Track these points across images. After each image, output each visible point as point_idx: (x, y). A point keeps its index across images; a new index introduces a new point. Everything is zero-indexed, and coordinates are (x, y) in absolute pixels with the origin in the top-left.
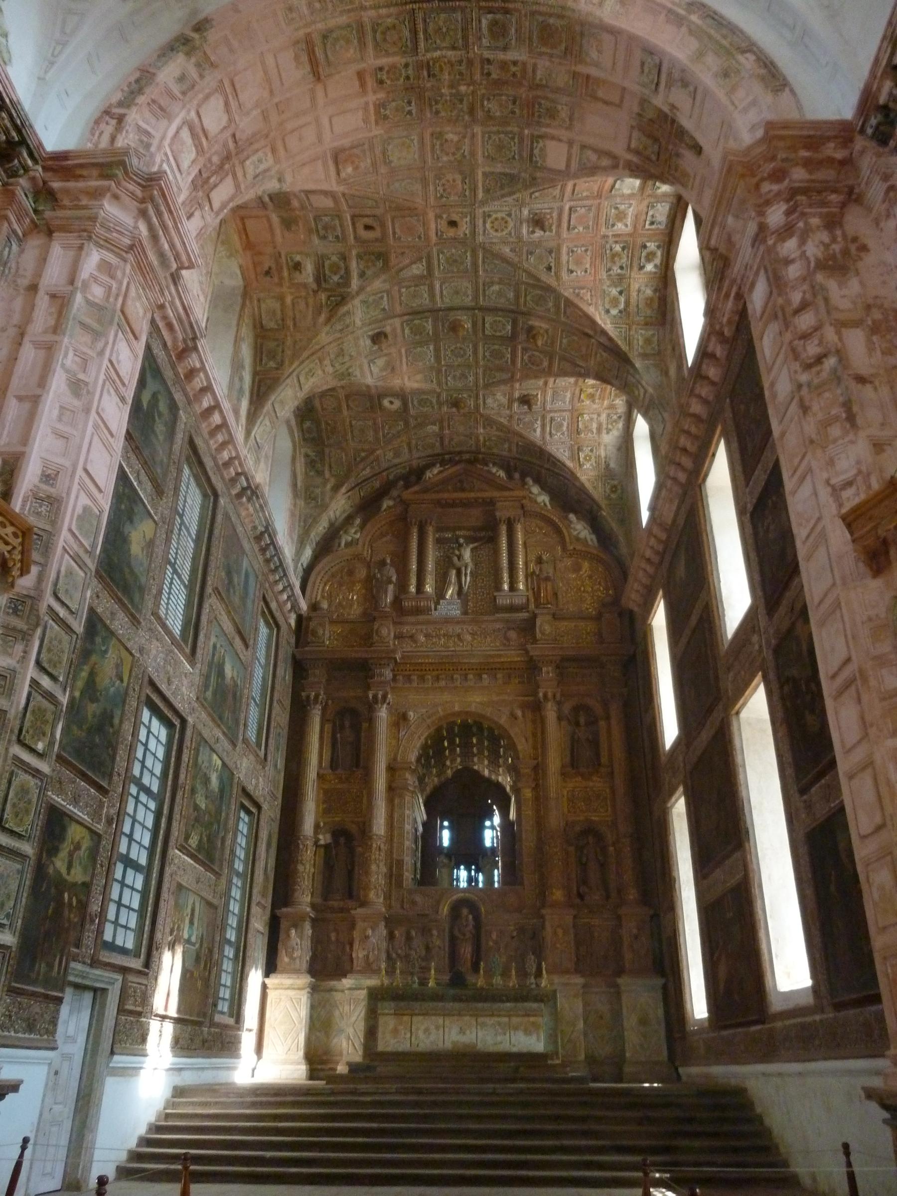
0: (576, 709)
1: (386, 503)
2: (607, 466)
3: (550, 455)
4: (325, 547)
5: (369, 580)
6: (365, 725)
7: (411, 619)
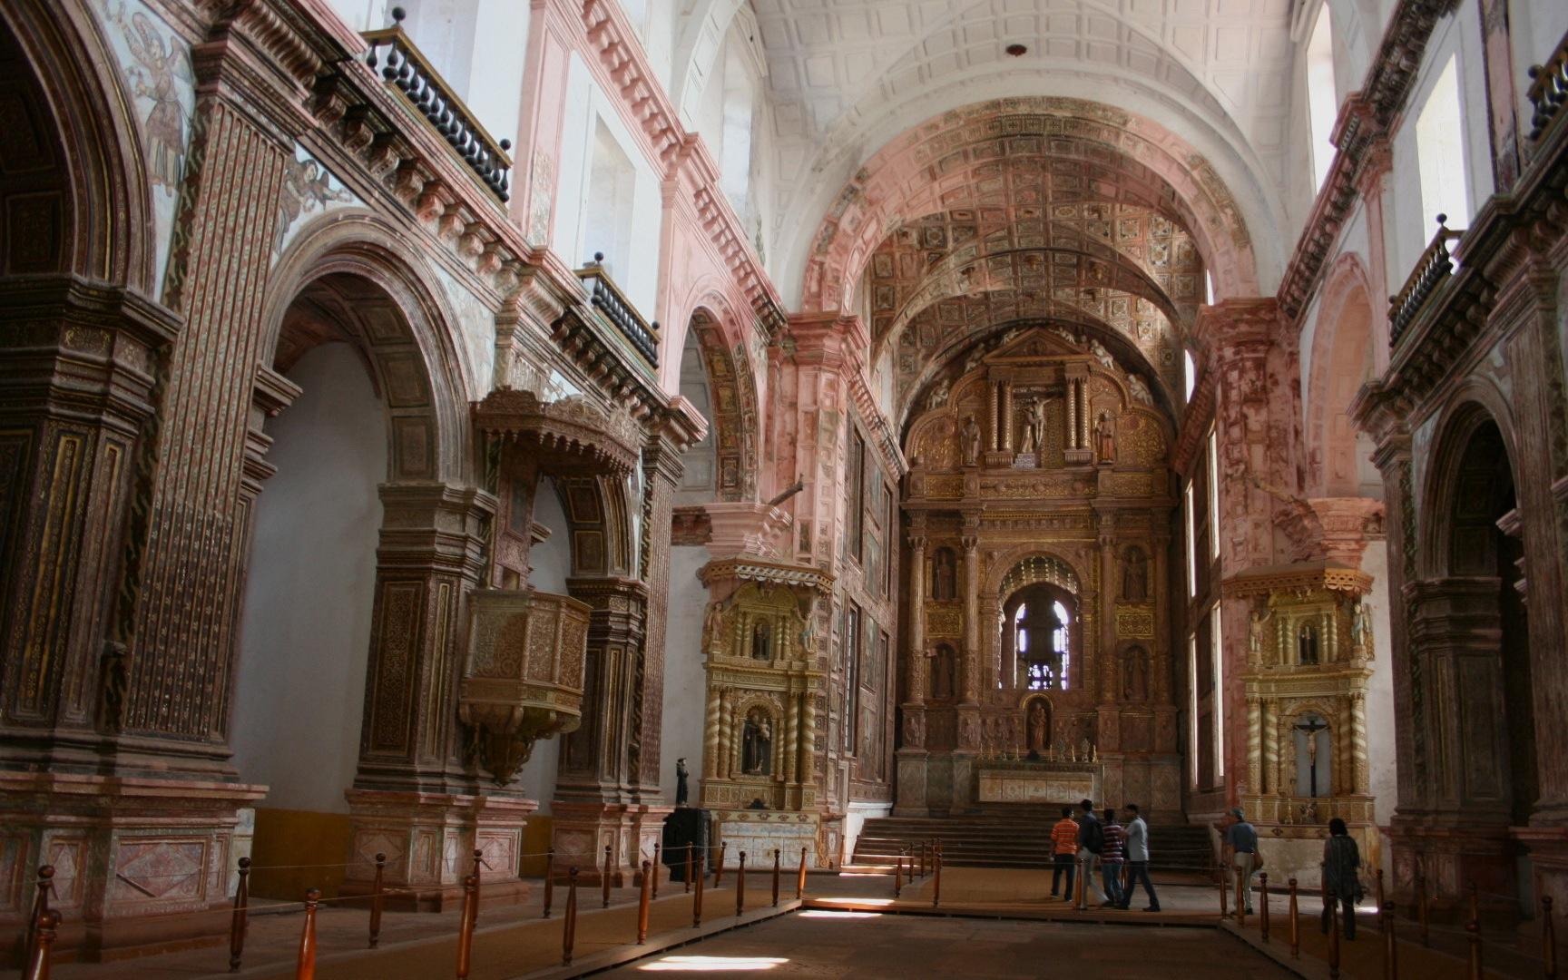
0: (1131, 548)
1: (970, 365)
2: (1163, 337)
4: (919, 407)
5: (957, 435)
7: (992, 472)
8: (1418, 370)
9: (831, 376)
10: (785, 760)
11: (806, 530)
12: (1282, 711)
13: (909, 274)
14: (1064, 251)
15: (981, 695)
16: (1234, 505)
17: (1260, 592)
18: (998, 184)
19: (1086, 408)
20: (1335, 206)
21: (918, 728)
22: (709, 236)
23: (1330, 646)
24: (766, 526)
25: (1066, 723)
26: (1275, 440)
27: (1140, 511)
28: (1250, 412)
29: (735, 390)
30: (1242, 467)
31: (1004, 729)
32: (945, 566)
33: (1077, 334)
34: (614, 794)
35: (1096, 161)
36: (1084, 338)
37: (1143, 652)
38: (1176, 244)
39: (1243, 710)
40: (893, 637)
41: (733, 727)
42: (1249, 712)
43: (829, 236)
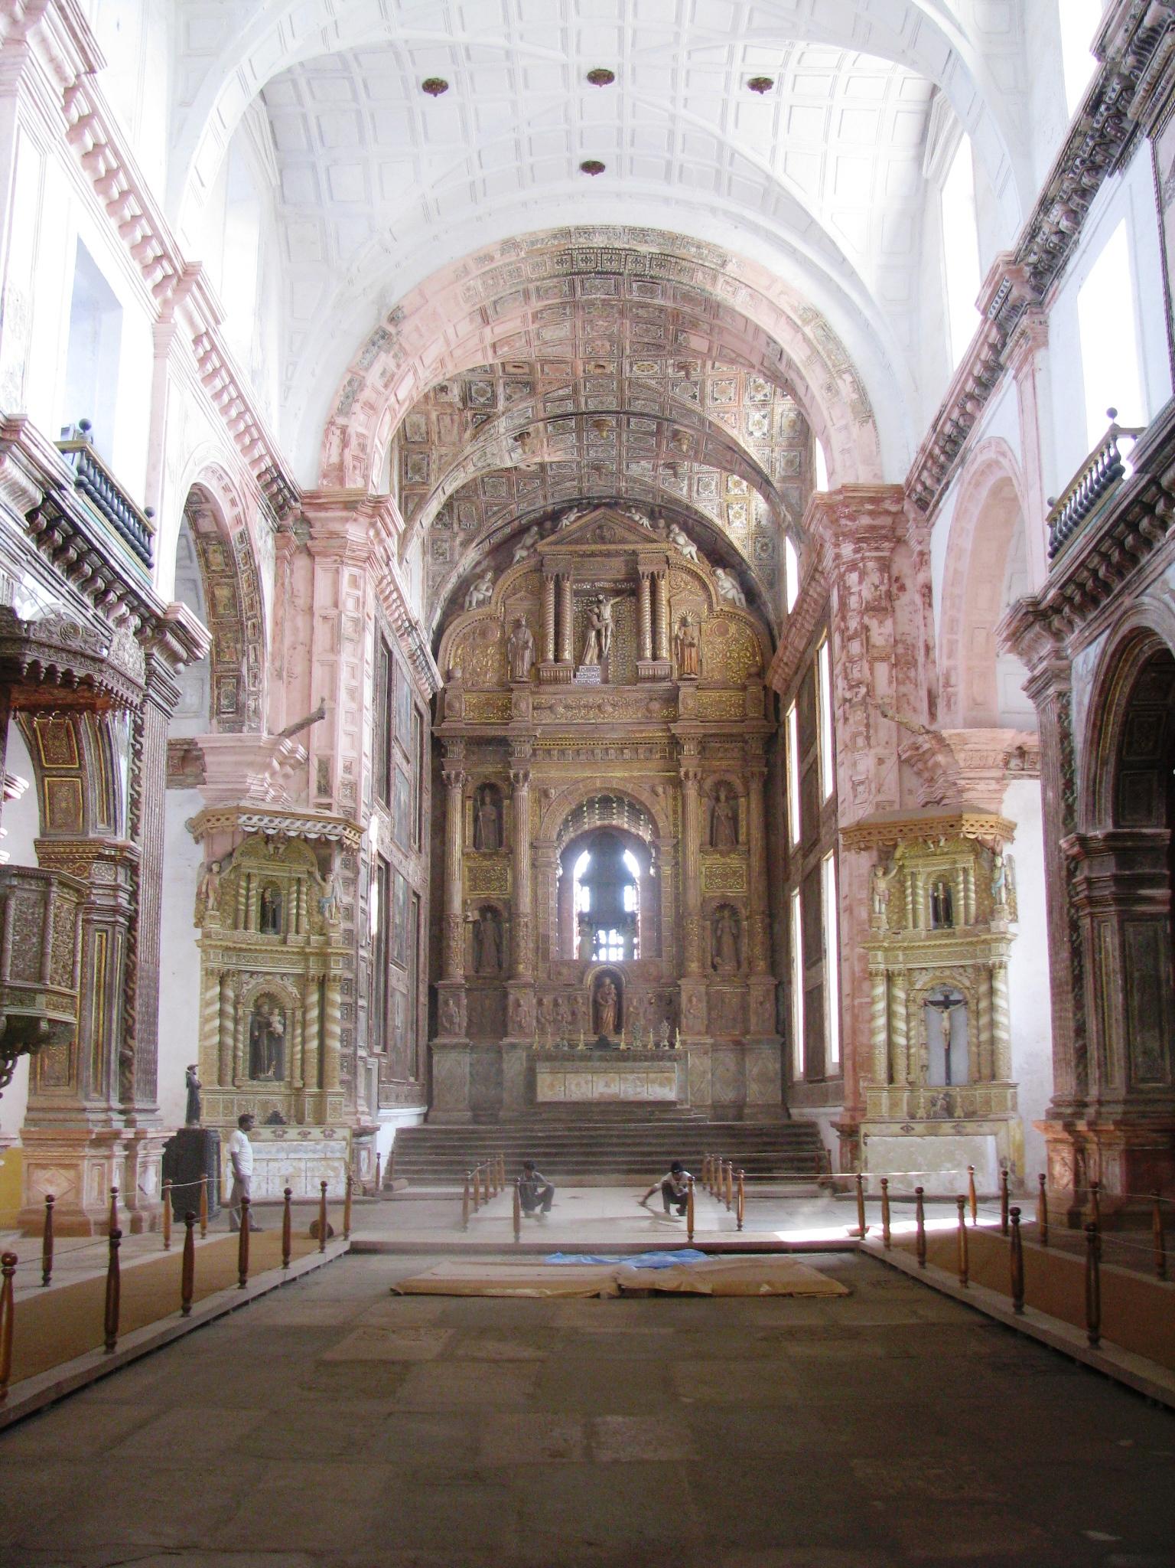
0: (719, 784)
1: (520, 553)
3: (696, 512)
5: (504, 641)
6: (506, 802)
7: (550, 689)
8: (1081, 586)
9: (355, 571)
10: (303, 1060)
11: (325, 768)
12: (912, 983)
13: (447, 439)
14: (642, 415)
15: (535, 968)
16: (854, 736)
17: (885, 841)
18: (563, 331)
19: (664, 609)
20: (978, 381)
21: (457, 1011)
22: (208, 392)
23: (967, 906)
24: (275, 764)
25: (641, 1000)
26: (904, 658)
27: (729, 737)
28: (873, 624)
29: (235, 589)
30: (863, 690)
31: (564, 1009)
32: (489, 809)
33: (652, 516)
34: (102, 1116)
35: (687, 309)
36: (662, 523)
37: (734, 912)
38: (778, 410)
39: (866, 985)
40: (425, 897)
41: (236, 1021)
42: (873, 987)
43: (351, 391)
